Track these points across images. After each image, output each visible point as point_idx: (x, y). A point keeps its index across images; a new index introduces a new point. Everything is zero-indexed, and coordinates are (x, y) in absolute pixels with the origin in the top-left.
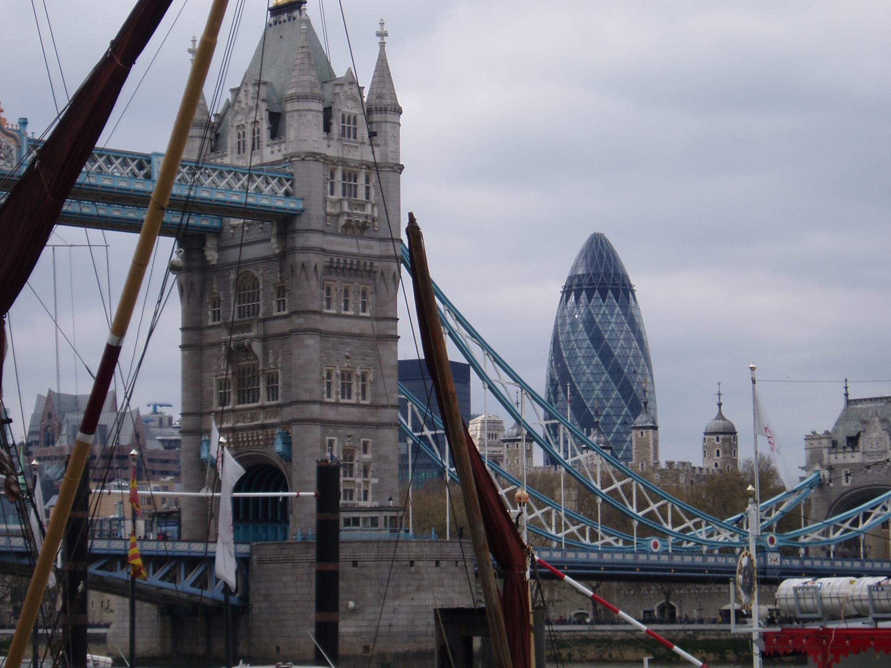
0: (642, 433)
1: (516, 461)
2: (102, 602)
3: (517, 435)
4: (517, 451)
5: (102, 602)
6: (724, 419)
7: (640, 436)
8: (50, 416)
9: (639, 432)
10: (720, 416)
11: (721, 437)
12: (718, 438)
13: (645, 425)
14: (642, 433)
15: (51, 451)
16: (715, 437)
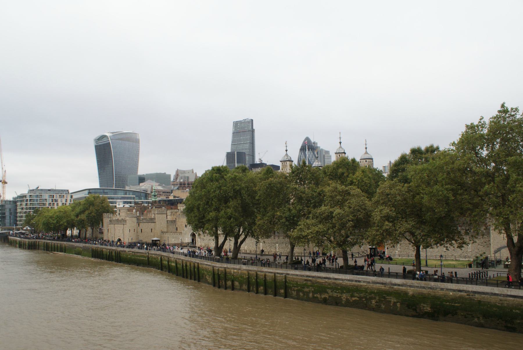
0: (339, 155)
1: (286, 170)
2: (108, 230)
3: (286, 159)
4: (286, 165)
5: (108, 230)
6: (368, 154)
7: (338, 156)
8: (178, 175)
9: (338, 155)
10: (366, 153)
11: (367, 160)
12: (366, 161)
13: (341, 152)
14: (339, 155)
15: (175, 183)
16: (365, 161)
